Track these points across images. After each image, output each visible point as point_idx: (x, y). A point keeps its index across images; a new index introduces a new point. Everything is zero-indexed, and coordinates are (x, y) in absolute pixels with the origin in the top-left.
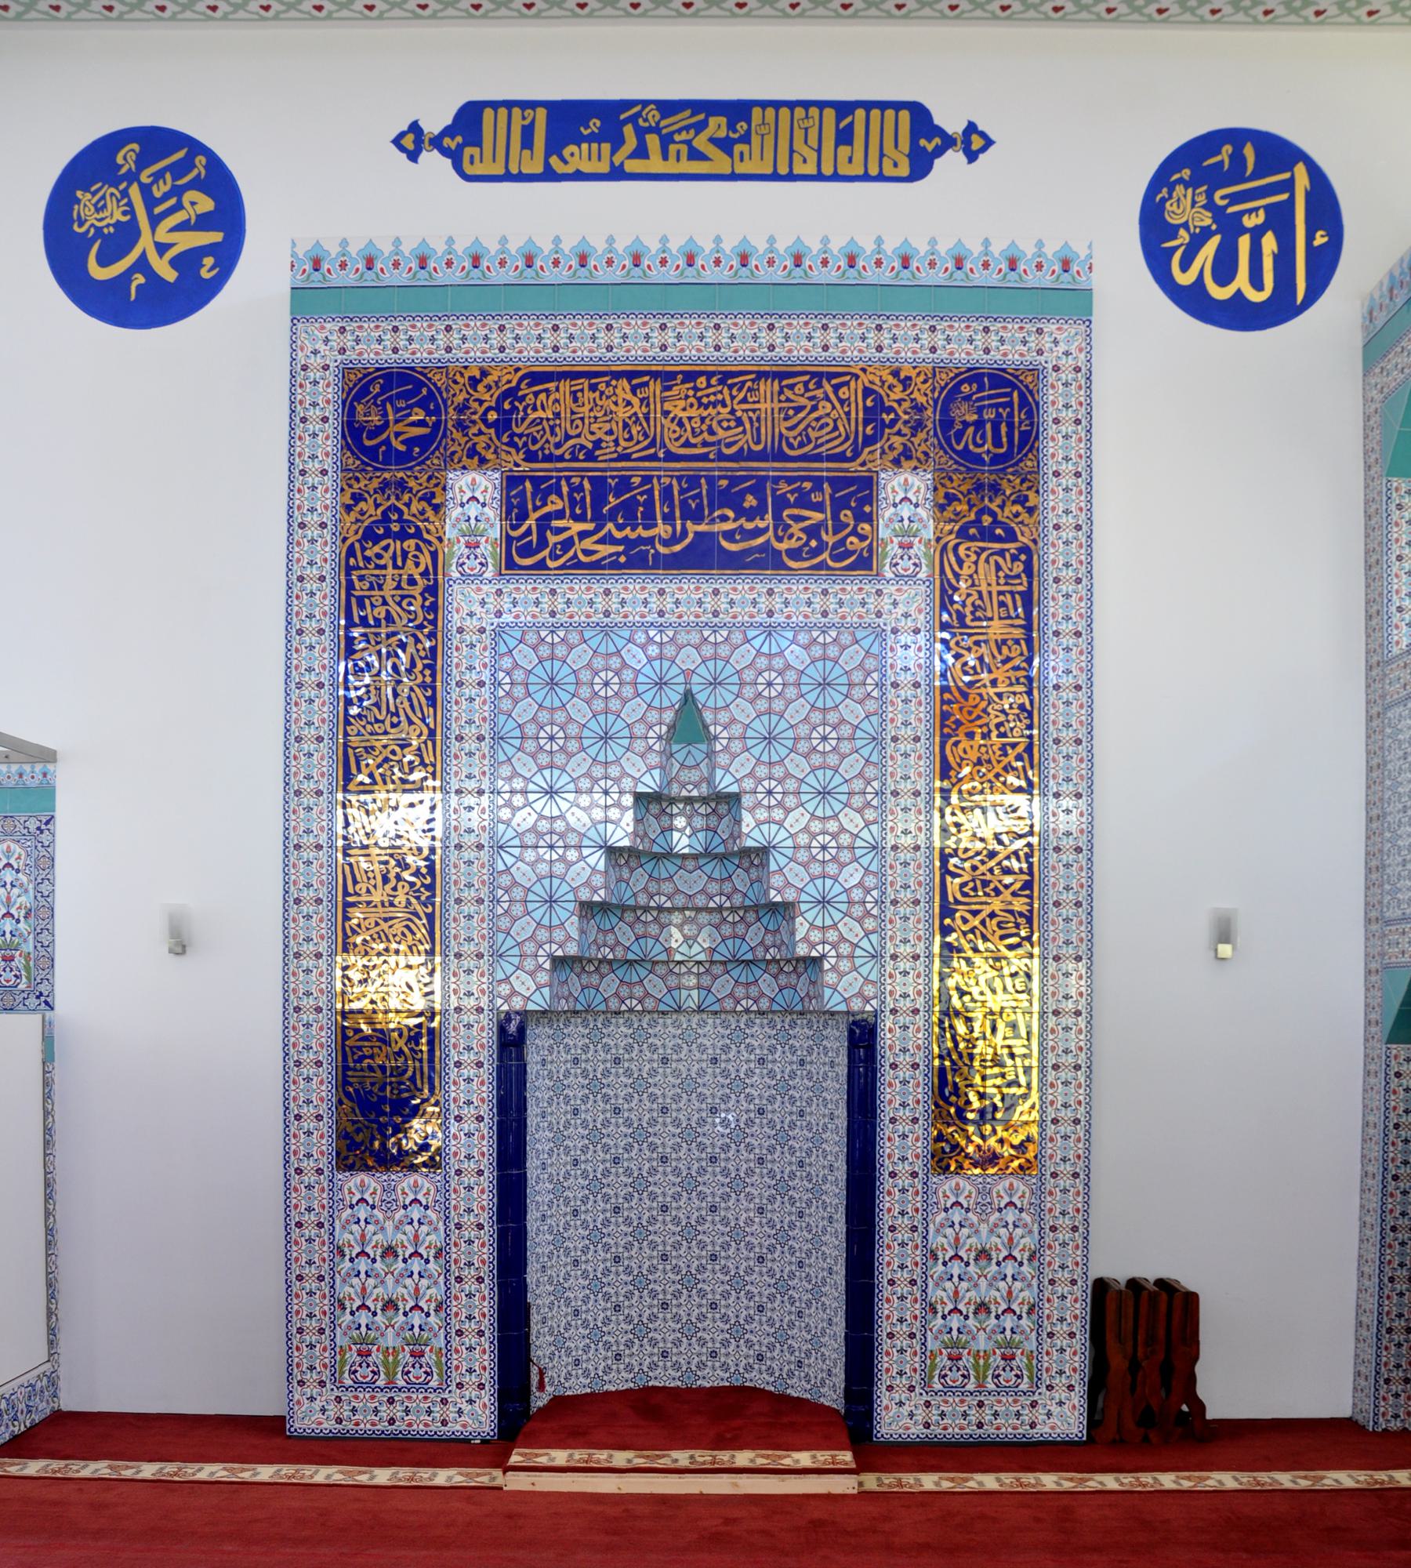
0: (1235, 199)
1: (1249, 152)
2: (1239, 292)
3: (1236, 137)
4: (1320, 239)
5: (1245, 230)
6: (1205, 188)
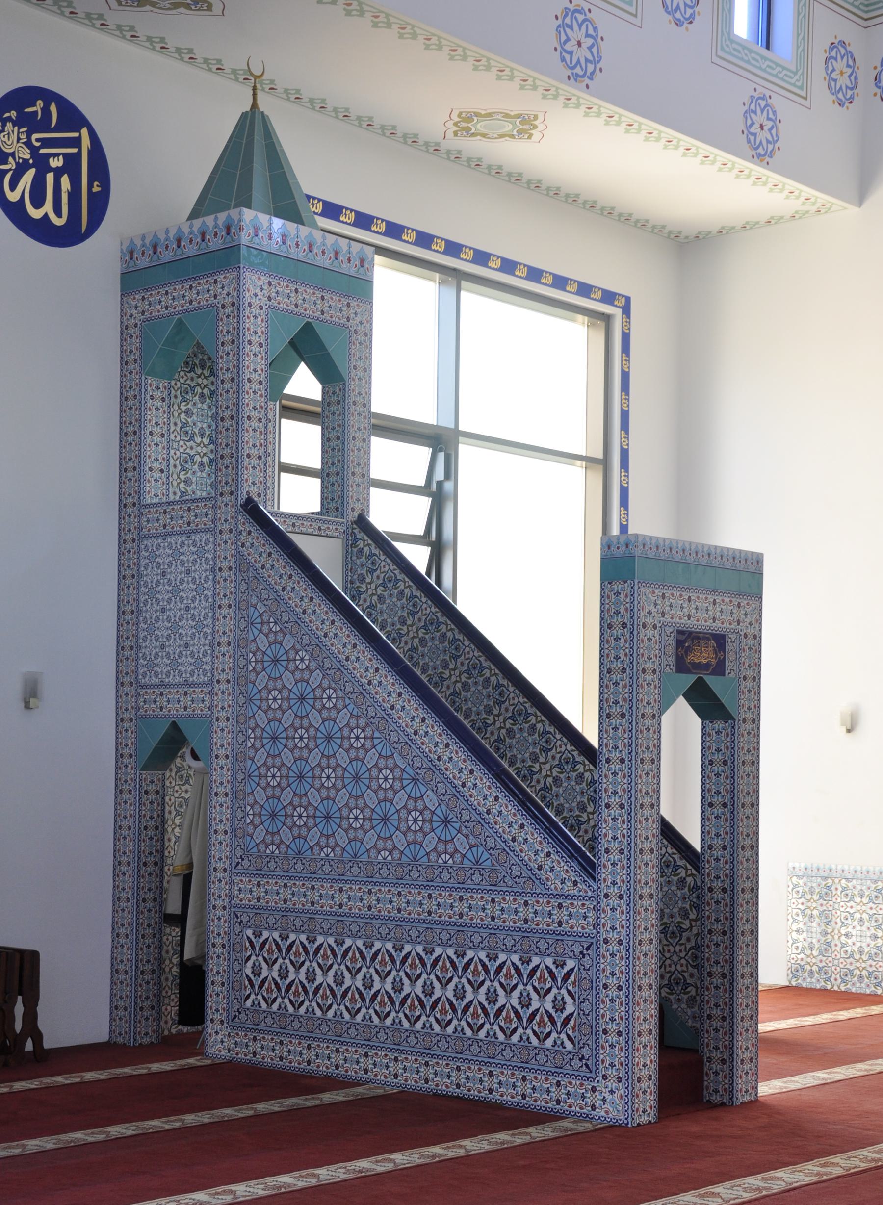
0: (46, 143)
1: (53, 108)
2: (46, 215)
3: (48, 96)
4: (96, 189)
5: (51, 169)
6: (26, 129)
